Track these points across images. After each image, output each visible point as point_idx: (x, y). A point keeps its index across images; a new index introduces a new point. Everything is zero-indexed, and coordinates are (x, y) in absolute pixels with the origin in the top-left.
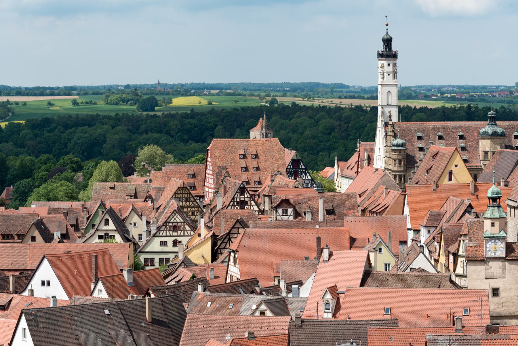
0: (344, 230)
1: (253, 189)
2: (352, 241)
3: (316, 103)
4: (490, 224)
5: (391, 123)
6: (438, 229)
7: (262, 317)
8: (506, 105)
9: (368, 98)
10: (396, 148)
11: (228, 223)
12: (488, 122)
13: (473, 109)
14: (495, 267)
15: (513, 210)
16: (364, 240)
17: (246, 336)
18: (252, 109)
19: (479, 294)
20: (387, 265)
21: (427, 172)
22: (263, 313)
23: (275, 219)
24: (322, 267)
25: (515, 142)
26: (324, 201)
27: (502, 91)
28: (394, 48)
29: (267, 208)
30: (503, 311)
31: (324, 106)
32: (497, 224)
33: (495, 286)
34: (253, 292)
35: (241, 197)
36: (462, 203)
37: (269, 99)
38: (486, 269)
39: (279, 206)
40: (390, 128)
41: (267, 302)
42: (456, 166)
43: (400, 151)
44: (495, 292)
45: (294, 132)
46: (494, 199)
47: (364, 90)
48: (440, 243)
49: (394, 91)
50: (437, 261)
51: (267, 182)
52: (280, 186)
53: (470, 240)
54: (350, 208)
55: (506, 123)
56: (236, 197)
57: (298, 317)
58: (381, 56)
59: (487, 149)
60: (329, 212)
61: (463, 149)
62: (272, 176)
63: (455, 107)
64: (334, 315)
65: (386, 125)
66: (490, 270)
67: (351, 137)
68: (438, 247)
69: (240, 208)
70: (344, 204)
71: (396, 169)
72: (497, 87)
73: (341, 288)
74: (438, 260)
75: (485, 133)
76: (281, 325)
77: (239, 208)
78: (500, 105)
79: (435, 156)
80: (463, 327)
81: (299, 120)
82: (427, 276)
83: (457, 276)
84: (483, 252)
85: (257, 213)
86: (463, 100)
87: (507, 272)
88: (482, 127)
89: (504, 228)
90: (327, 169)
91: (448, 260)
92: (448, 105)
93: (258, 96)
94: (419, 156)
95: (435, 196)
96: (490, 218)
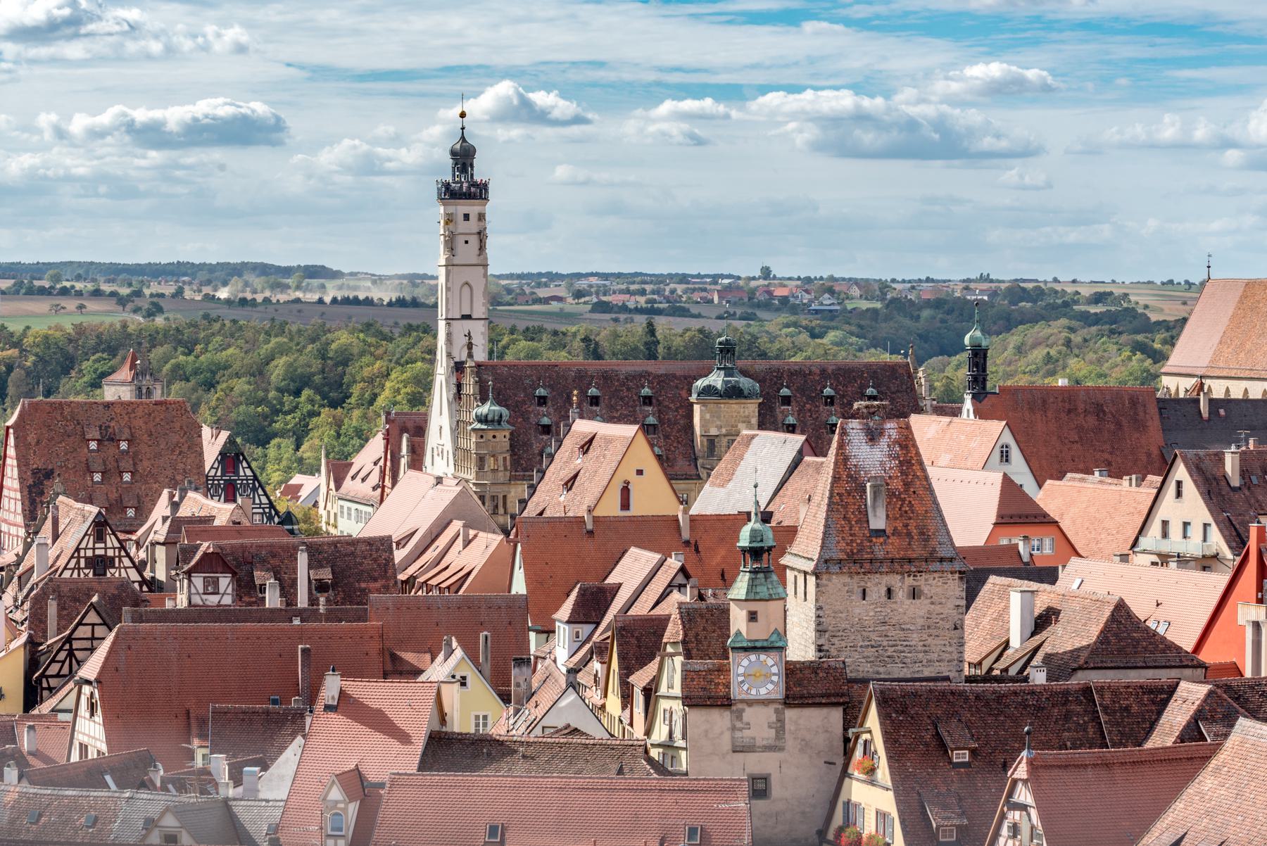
11: (65, 612)
23: (185, 604)
25: (782, 412)
27: (728, 288)
35: (97, 545)
38: (734, 728)
42: (640, 472)
53: (688, 655)
54: (376, 574)
56: (83, 545)
59: (714, 432)
65: (459, 367)
66: (746, 733)
69: (95, 574)
70: (361, 564)
74: (603, 707)
77: (91, 575)
79: (586, 446)
84: (728, 686)
85: (136, 585)
86: (630, 311)
87: (787, 736)
88: (701, 377)
93: (113, 294)
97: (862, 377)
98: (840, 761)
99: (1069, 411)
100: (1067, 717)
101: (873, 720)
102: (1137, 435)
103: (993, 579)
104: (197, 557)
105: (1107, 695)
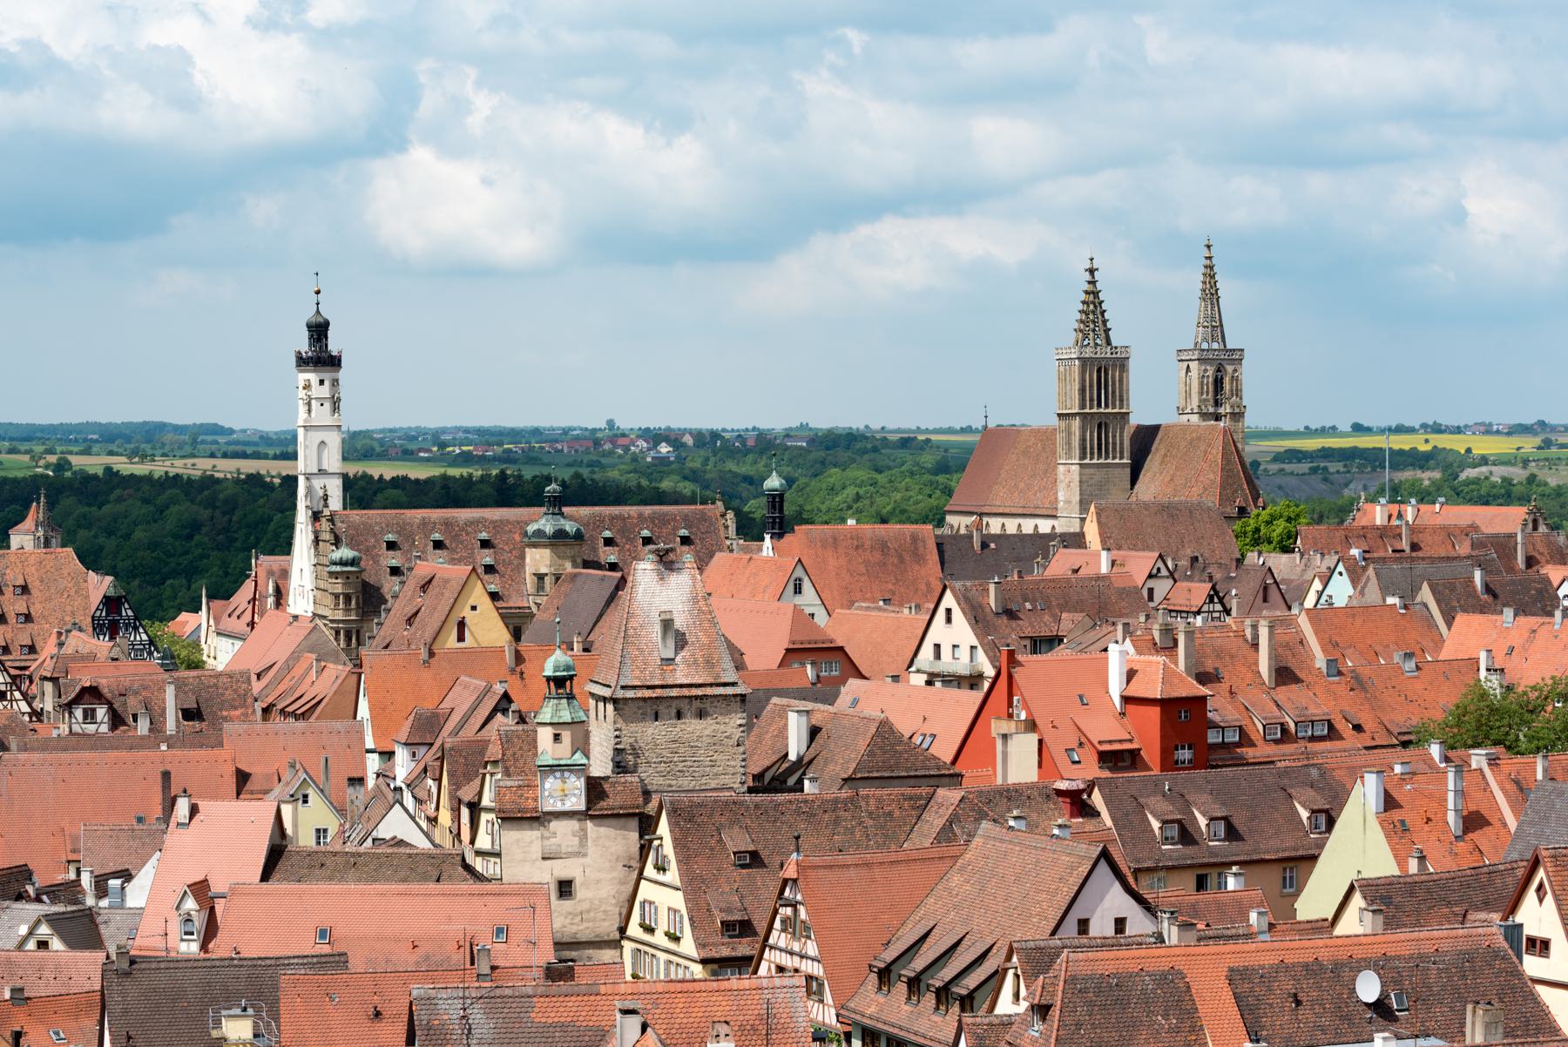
0: (224, 753)
1: (17, 664)
2: (242, 778)
3: (159, 468)
4: (551, 738)
5: (326, 512)
6: (434, 748)
7: (42, 953)
8: (585, 472)
9: (275, 457)
10: (338, 568)
12: (544, 509)
13: (511, 481)
14: (563, 831)
15: (601, 705)
16: (268, 777)
17: (7, 995)
18: (15, 481)
19: (528, 892)
20: (321, 833)
21: (410, 621)
22: (43, 945)
24: (173, 837)
26: (178, 689)
27: (577, 438)
28: (333, 346)
29: (48, 705)
30: (583, 931)
31: (177, 476)
32: (566, 736)
33: (565, 874)
34: (20, 897)
36: (488, 690)
37: (53, 459)
39: (76, 701)
40: (325, 525)
41: (51, 920)
43: (347, 575)
44: (565, 888)
45: (110, 533)
46: (559, 682)
47: (266, 439)
48: (439, 780)
49: (334, 441)
50: (433, 820)
51: (48, 649)
52: (78, 657)
53: (507, 773)
55: (585, 511)
57: (122, 952)
58: (302, 362)
59: (543, 570)
60: (189, 714)
61: (489, 569)
62: (60, 634)
63: (470, 475)
64: (204, 947)
65: (316, 516)
67: (238, 544)
68: (434, 790)
71: (339, 615)
72: (566, 431)
73: (217, 887)
75: (539, 533)
76: (83, 969)
78: (572, 471)
79: (425, 586)
80: (493, 968)
81: (120, 508)
82: (410, 856)
83: (479, 853)
84: (536, 800)
85: (27, 718)
89: (582, 745)
90: (184, 616)
91: (457, 817)
92: (455, 472)
94: (390, 585)
95: (426, 675)
96: (551, 724)
97: (674, 519)
98: (635, 864)
99: (857, 547)
100: (837, 821)
101: (663, 828)
102: (916, 567)
103: (775, 700)
104: (78, 689)
105: (872, 802)
